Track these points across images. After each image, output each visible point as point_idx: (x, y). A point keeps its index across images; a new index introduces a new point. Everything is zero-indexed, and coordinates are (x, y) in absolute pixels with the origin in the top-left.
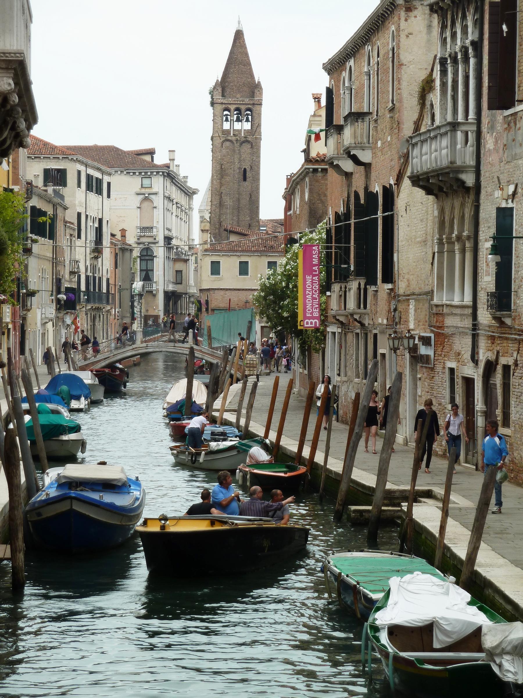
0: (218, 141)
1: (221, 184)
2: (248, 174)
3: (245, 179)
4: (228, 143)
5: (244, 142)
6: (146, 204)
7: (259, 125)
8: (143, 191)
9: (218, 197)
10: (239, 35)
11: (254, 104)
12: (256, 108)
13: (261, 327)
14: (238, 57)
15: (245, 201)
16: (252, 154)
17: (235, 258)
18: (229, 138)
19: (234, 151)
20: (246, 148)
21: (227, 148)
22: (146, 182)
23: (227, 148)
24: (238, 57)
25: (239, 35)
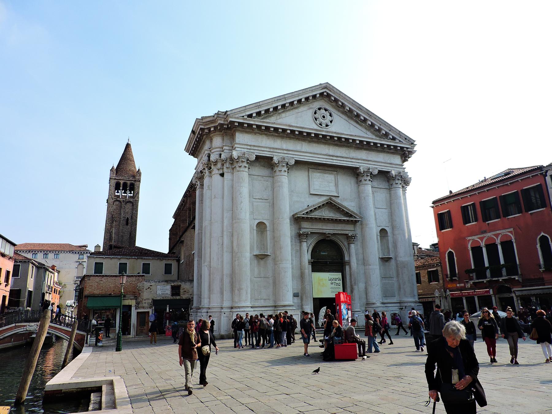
0: (111, 201)
1: (112, 227)
2: (130, 221)
3: (127, 224)
4: (117, 203)
5: (128, 202)
6: (80, 266)
7: (138, 193)
8: (79, 260)
9: (108, 234)
10: (128, 146)
11: (135, 181)
12: (136, 183)
13: (138, 312)
14: (127, 156)
15: (127, 237)
16: (133, 209)
17: (116, 260)
18: (118, 199)
19: (121, 207)
20: (129, 206)
21: (117, 205)
22: (81, 257)
23: (117, 205)
24: (127, 156)
25: (128, 146)
